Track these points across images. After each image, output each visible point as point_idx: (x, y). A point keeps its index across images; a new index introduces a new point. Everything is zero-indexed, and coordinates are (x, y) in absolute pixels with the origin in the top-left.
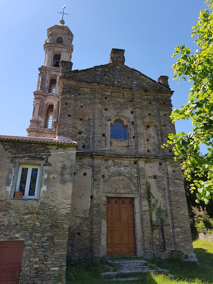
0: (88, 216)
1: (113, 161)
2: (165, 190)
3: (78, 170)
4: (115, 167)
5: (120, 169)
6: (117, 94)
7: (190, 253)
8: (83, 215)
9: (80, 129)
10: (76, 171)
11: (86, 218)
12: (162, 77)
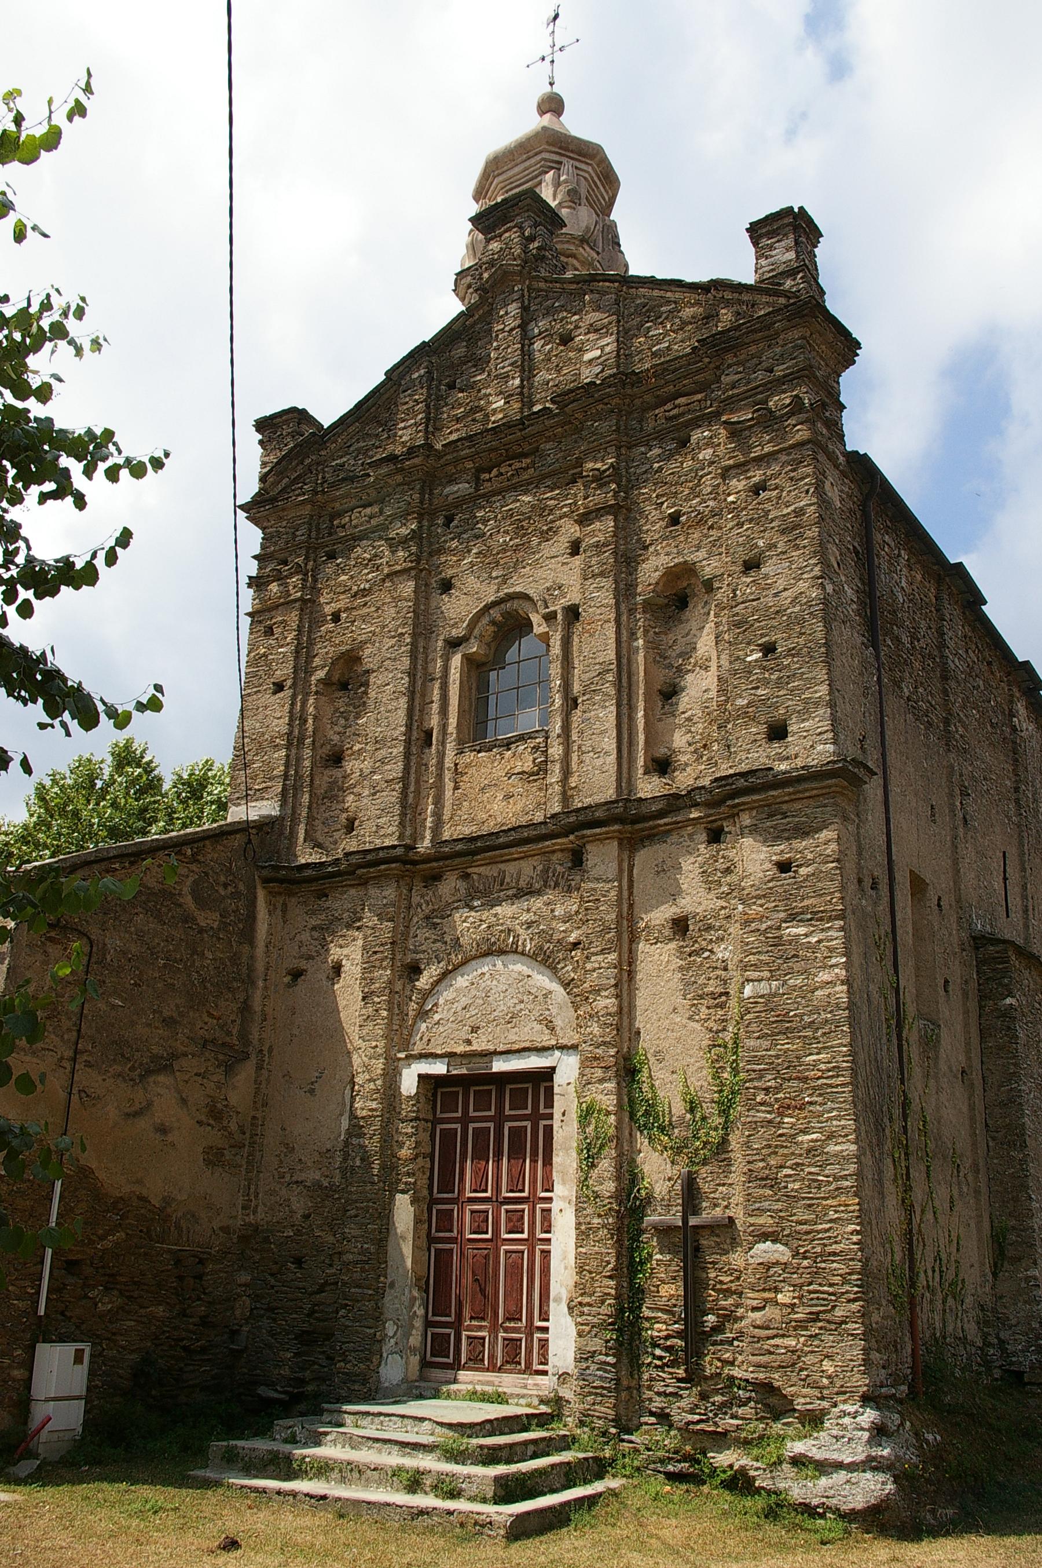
0: (337, 1180)
1: (466, 876)
2: (722, 1006)
3: (310, 958)
4: (472, 908)
5: (496, 915)
6: (502, 470)
7: (835, 1405)
8: (317, 1175)
9: (336, 738)
10: (303, 964)
11: (332, 1188)
12: (761, 231)
